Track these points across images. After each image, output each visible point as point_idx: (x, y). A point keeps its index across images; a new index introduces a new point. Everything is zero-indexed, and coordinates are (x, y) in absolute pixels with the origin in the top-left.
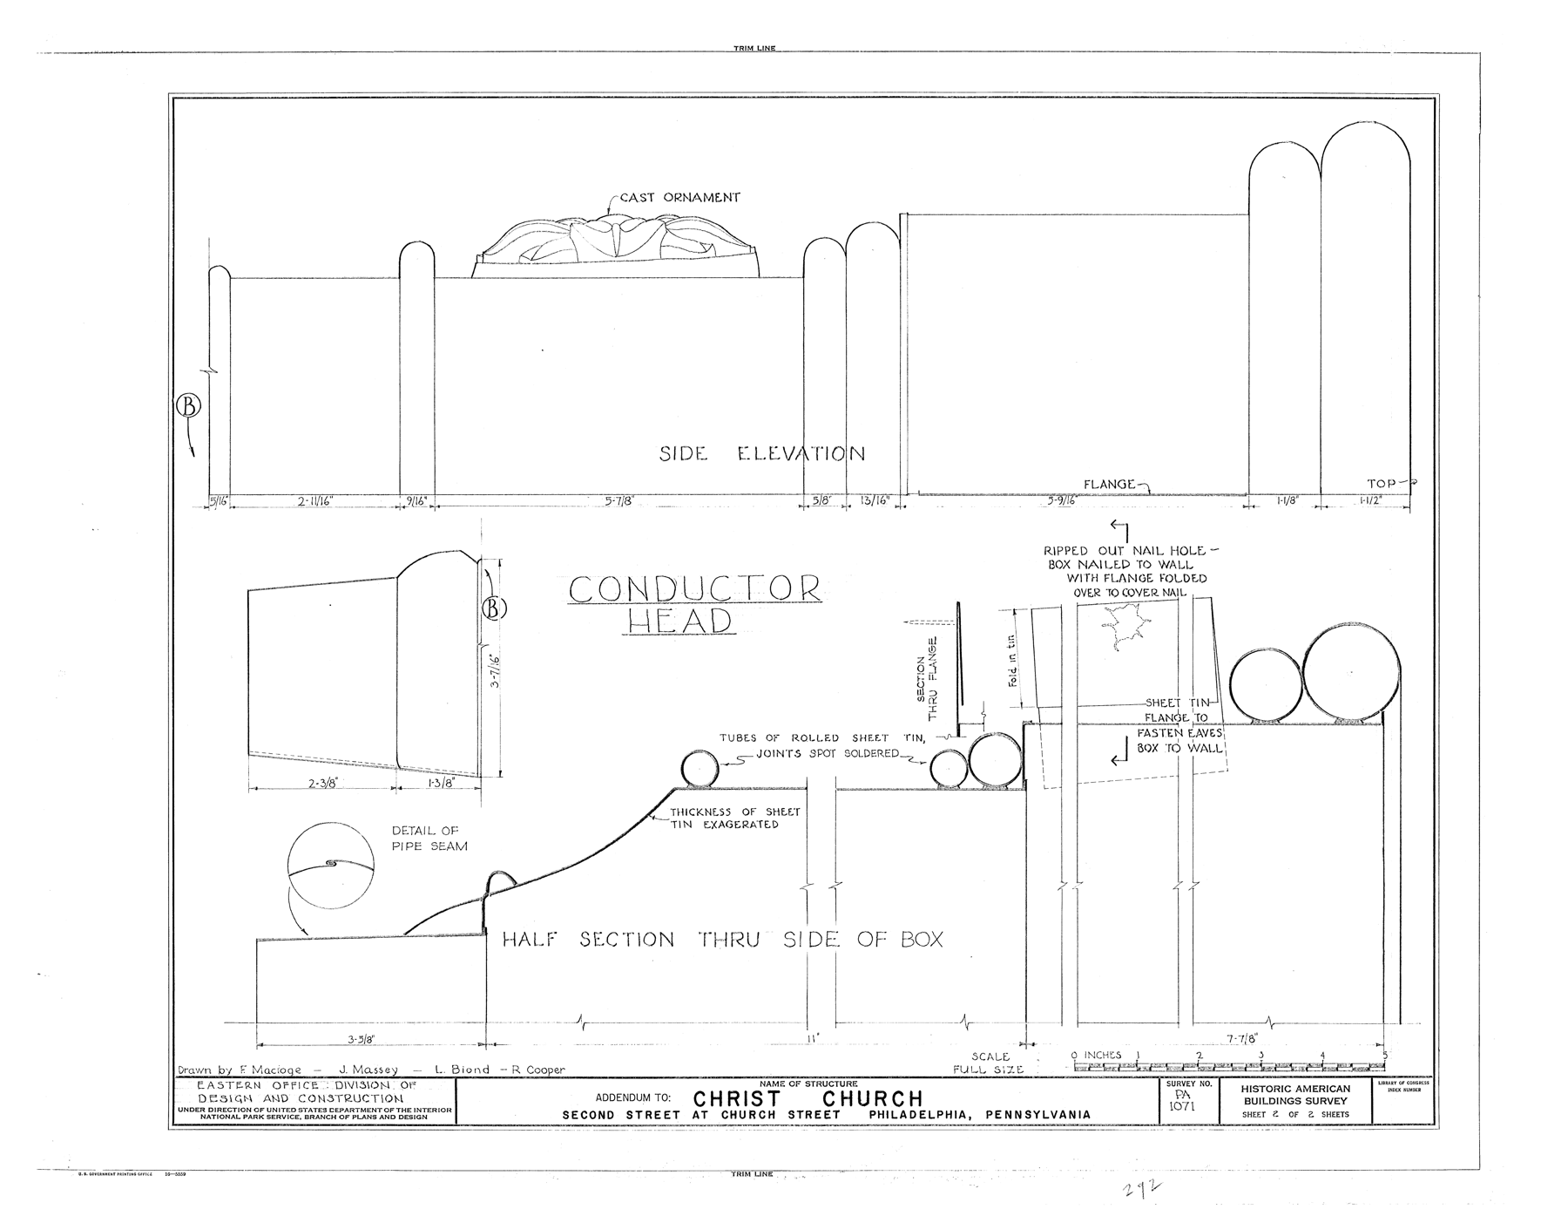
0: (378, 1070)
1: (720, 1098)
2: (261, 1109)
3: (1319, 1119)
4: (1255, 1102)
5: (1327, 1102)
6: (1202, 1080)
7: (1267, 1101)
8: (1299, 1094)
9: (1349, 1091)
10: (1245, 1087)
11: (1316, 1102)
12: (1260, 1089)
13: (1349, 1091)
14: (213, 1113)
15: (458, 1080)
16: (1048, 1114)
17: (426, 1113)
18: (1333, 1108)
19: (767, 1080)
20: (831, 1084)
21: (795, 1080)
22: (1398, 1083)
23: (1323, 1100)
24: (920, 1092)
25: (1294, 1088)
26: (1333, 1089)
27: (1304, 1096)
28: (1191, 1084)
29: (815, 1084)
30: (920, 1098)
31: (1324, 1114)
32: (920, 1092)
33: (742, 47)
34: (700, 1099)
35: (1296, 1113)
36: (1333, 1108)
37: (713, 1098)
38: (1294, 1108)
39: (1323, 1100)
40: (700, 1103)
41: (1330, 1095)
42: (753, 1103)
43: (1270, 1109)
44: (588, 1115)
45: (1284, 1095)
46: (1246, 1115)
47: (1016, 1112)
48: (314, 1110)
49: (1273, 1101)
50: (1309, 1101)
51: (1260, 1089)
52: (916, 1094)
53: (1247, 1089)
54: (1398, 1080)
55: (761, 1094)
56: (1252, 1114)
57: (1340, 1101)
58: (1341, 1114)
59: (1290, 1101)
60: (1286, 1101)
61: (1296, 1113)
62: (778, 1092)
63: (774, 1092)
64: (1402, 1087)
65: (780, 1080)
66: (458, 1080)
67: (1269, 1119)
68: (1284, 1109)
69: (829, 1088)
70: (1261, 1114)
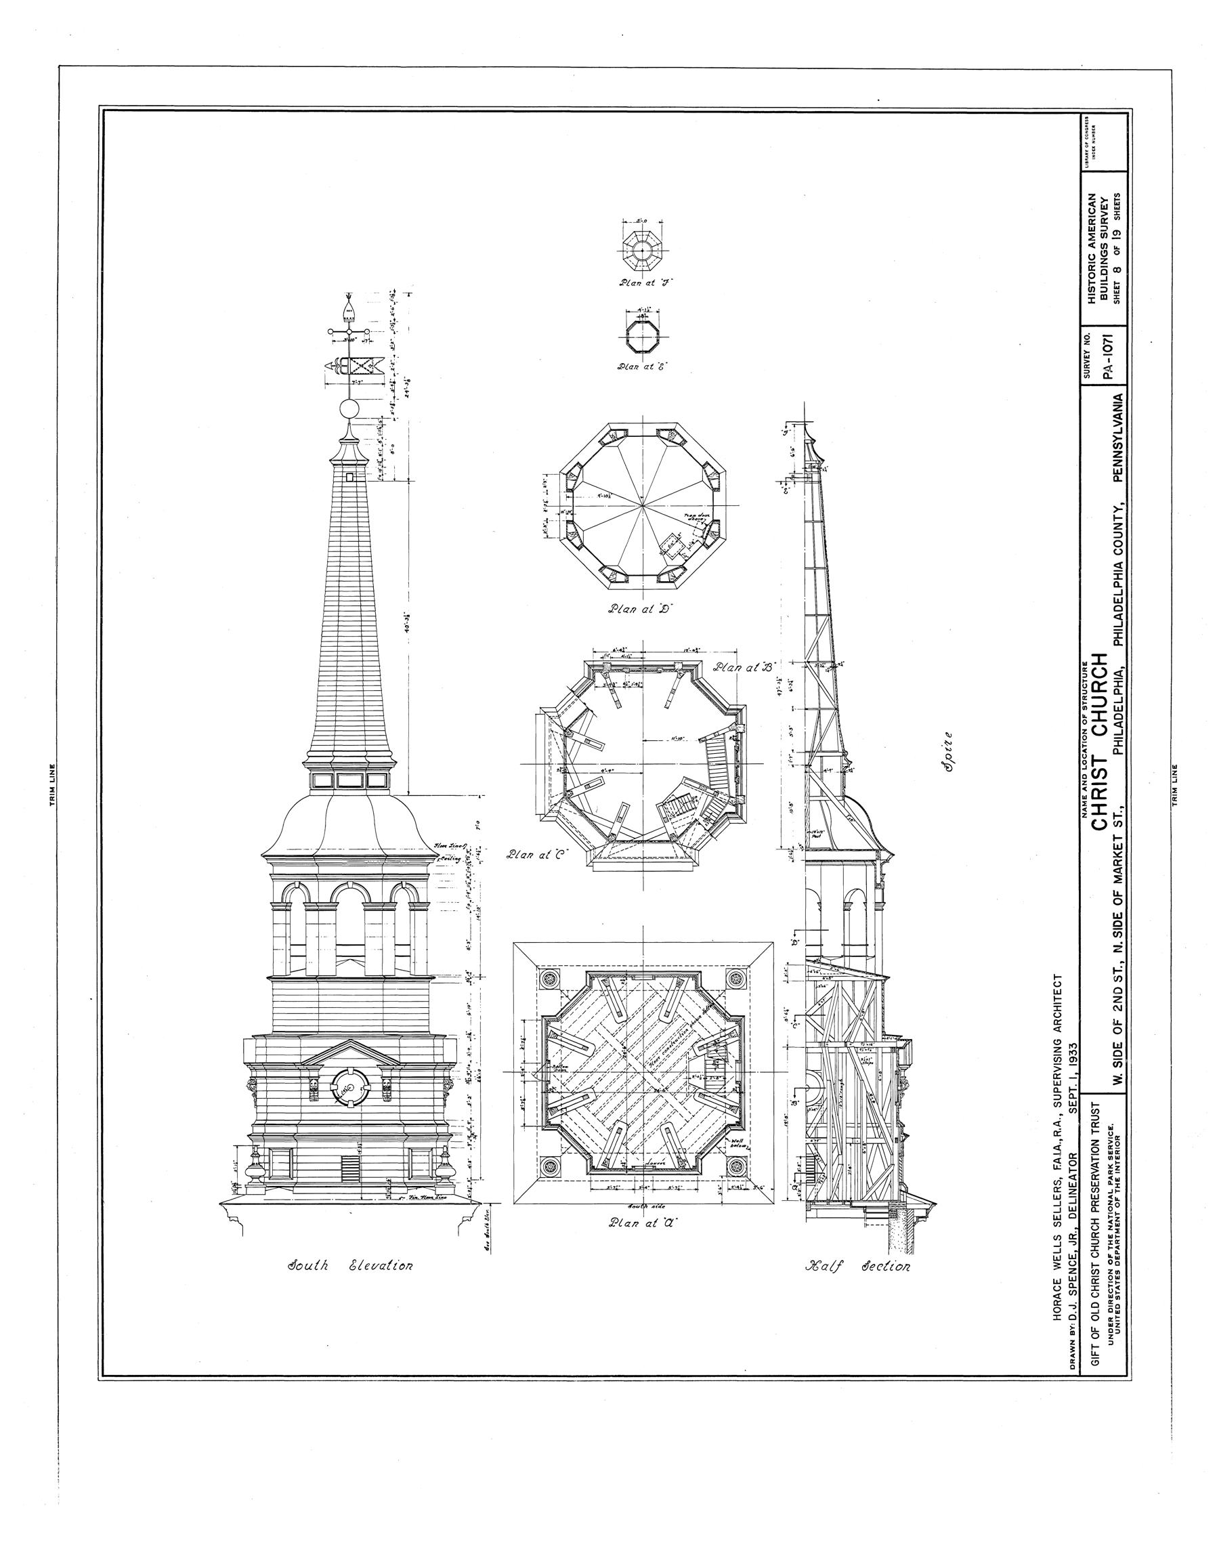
0: (1072, 1049)
1: (1099, 806)
2: (1110, 1256)
3: (1121, 225)
4: (1105, 290)
5: (1105, 217)
6: (1083, 342)
7: (1104, 278)
8: (1097, 245)
9: (1094, 195)
10: (1090, 300)
11: (1105, 228)
12: (1092, 285)
13: (1094, 195)
14: (1114, 1308)
15: (1082, 324)
16: (1118, 429)
17: (1114, 1136)
18: (1111, 211)
19: (1082, 812)
20: (1085, 686)
21: (1082, 719)
22: (1087, 149)
23: (1104, 221)
24: (1093, 655)
25: (1091, 251)
26: (1092, 211)
27: (1099, 241)
28: (1087, 354)
29: (1085, 701)
30: (1099, 656)
31: (1117, 217)
32: (1093, 655)
33: (52, 799)
34: (1099, 824)
35: (1116, 248)
36: (1111, 211)
37: (1099, 813)
38: (1111, 250)
39: (1104, 221)
40: (1103, 824)
41: (1098, 214)
42: (1104, 778)
43: (1112, 277)
44: (1118, 549)
45: (1098, 260)
46: (1117, 301)
47: (1115, 528)
48: (1111, 1219)
49: (1104, 272)
50: (1104, 235)
51: (1092, 285)
52: (1093, 300)
53: (1091, 298)
54: (1084, 149)
55: (1095, 770)
56: (1117, 293)
57: (1104, 204)
58: (1117, 201)
59: (1104, 255)
60: (1104, 259)
61: (1116, 248)
62: (1093, 756)
63: (1093, 761)
64: (1091, 145)
65: (1082, 800)
66: (1081, 1092)
67: (1121, 278)
68: (1114, 261)
69: (1089, 732)
70: (1117, 285)
